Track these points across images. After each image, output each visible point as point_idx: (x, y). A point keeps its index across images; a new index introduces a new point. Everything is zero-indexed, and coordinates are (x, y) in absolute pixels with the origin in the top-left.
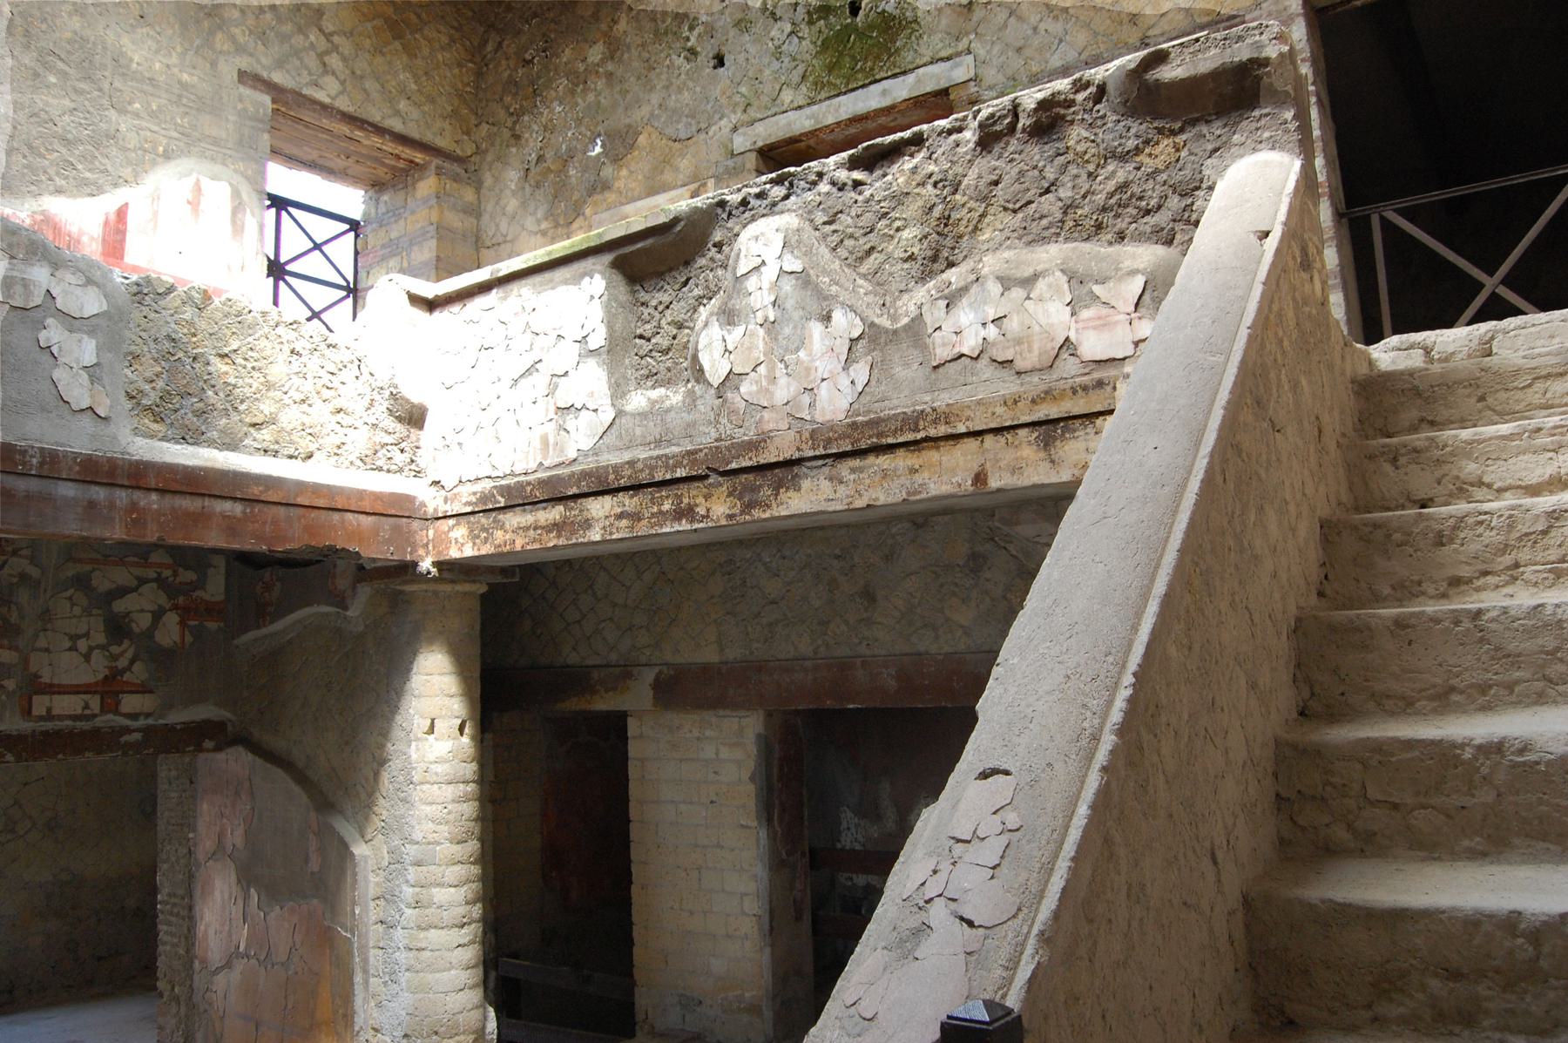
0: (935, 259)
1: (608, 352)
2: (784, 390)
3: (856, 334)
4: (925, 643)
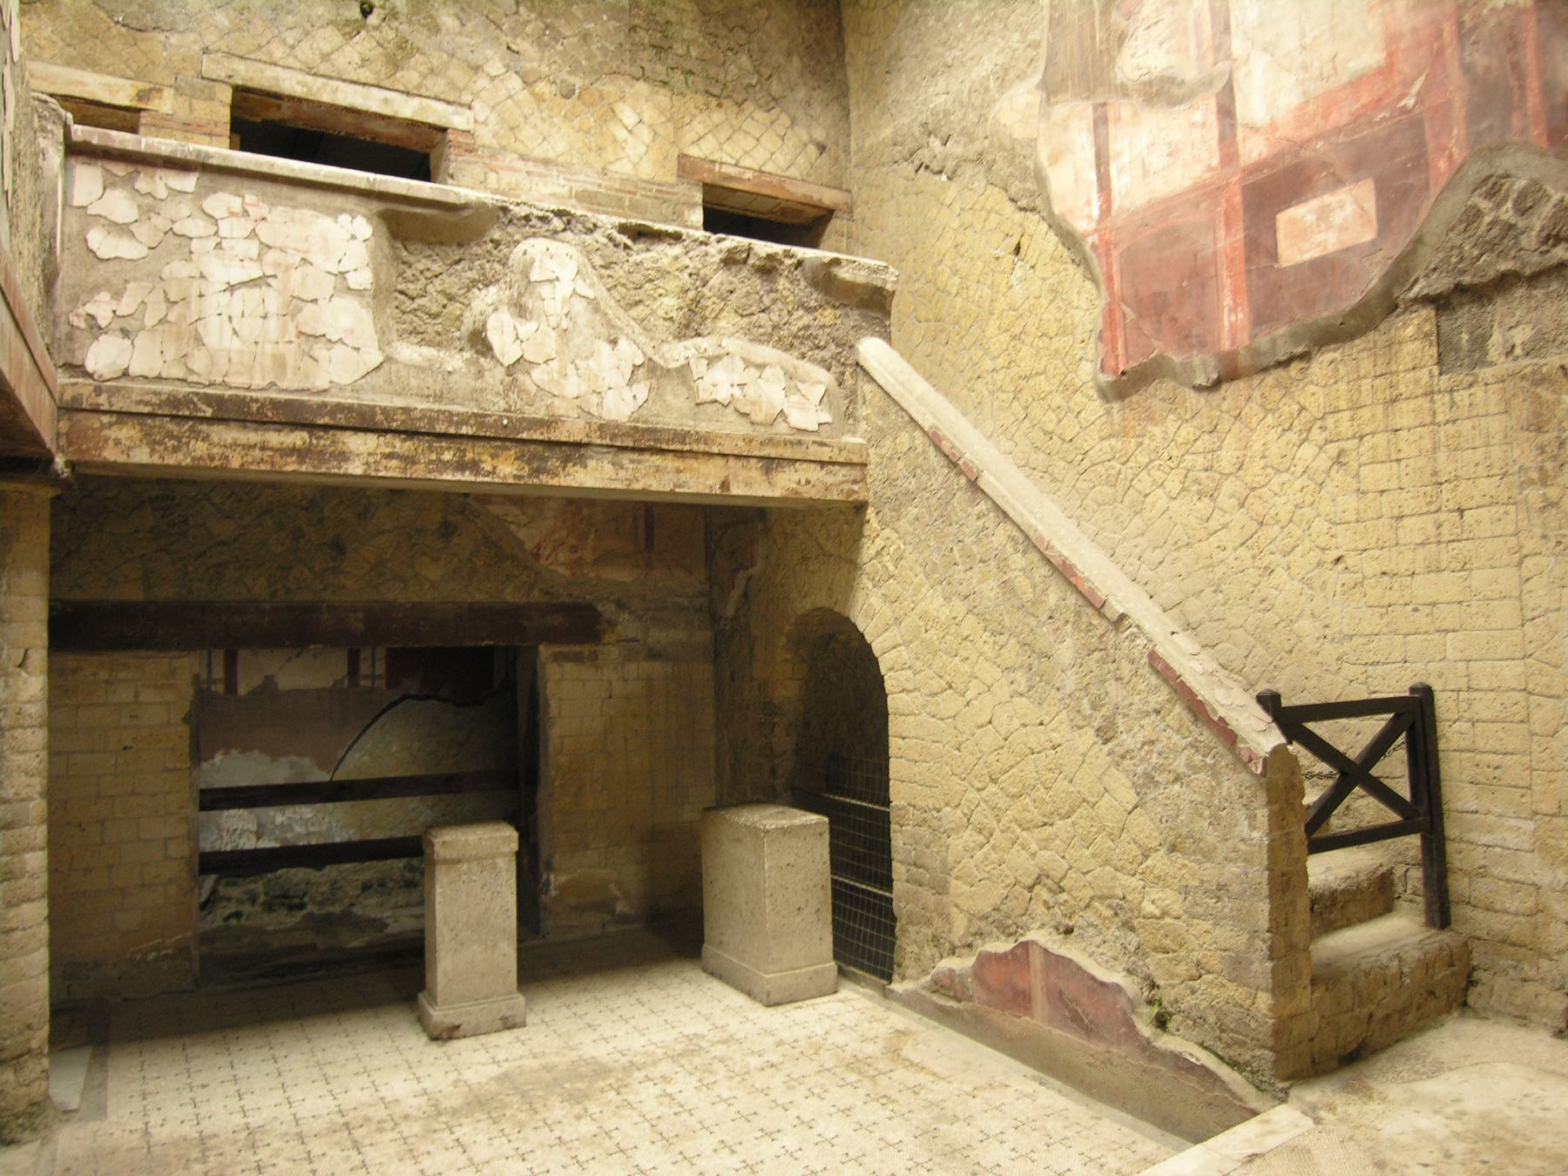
0: (687, 326)
1: (375, 297)
2: (573, 387)
3: (639, 362)
4: (395, 593)
